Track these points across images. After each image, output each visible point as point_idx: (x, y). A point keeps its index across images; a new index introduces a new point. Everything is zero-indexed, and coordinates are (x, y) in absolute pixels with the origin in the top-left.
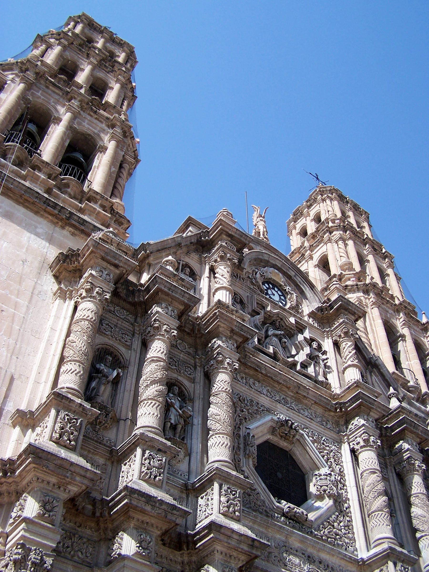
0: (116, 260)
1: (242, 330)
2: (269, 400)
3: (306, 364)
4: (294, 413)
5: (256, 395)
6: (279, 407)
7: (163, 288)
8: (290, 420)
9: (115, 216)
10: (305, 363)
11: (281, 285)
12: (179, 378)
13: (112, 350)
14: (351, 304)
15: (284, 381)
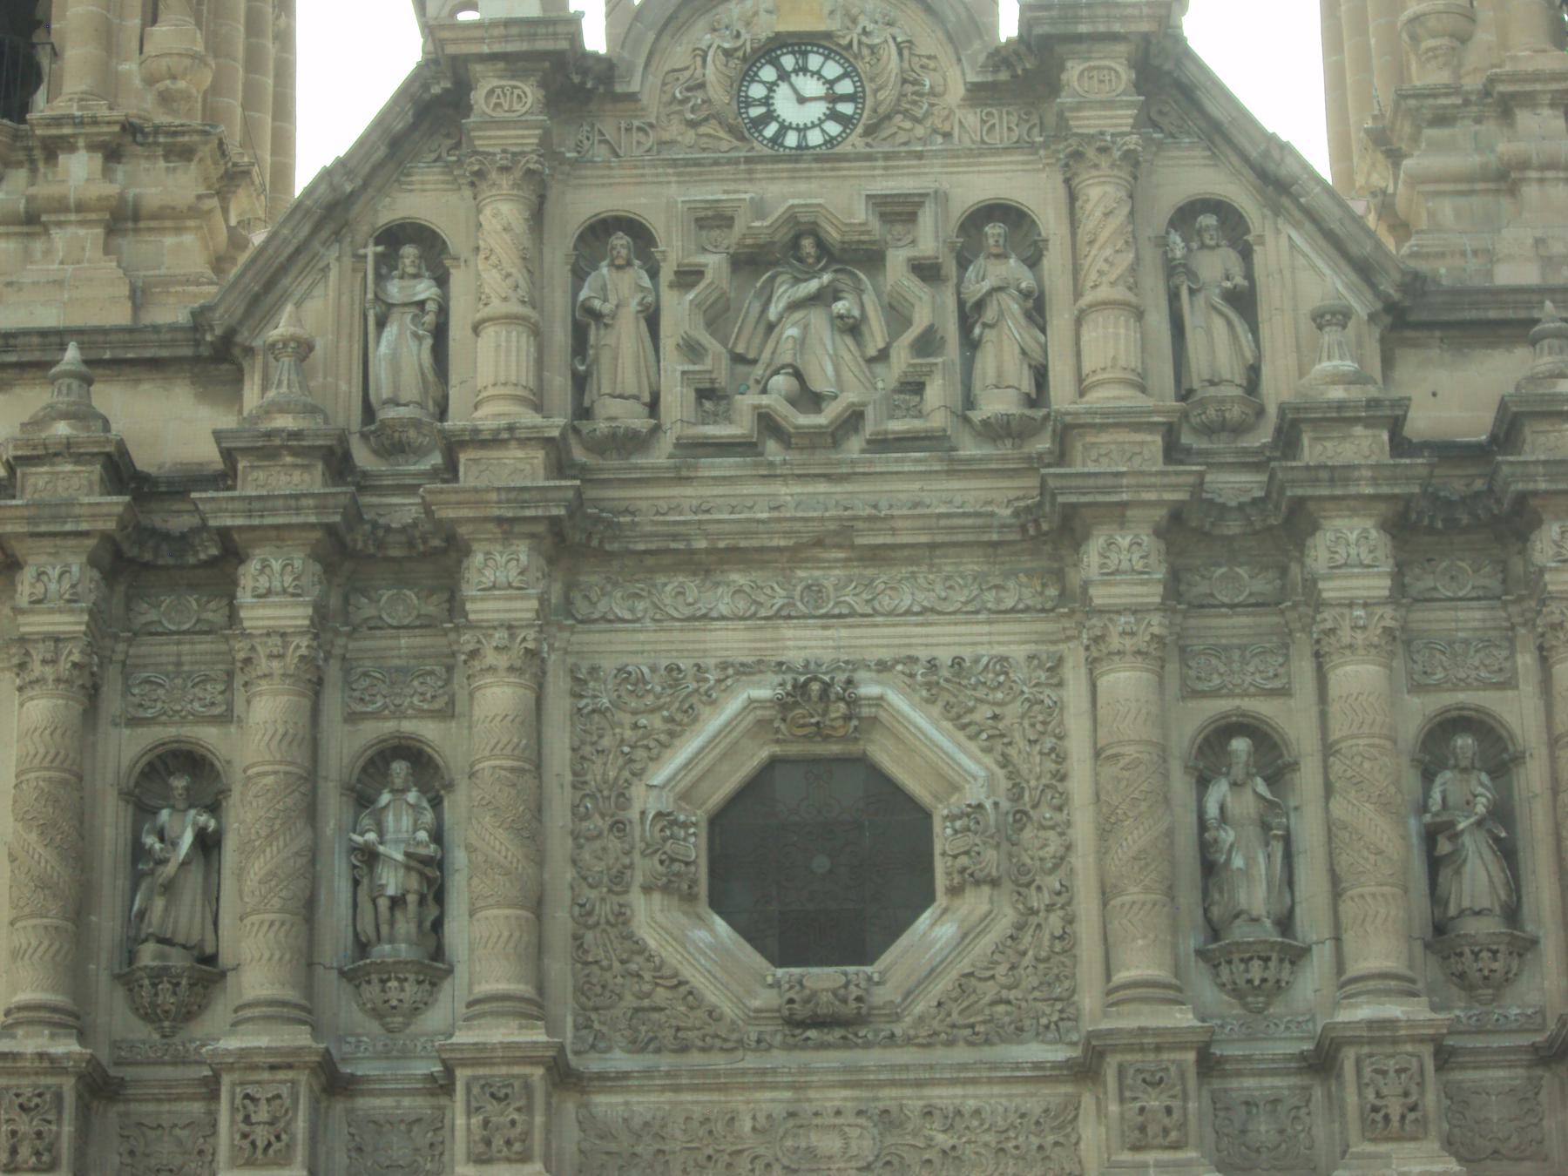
0: (65, 523)
1: (524, 504)
2: (748, 629)
3: (917, 379)
4: (850, 626)
5: (691, 636)
6: (789, 633)
7: (229, 522)
8: (815, 679)
9: (157, 144)
10: (910, 379)
11: (828, 35)
12: (408, 726)
13: (185, 747)
14: (1084, 12)
15: (788, 534)
